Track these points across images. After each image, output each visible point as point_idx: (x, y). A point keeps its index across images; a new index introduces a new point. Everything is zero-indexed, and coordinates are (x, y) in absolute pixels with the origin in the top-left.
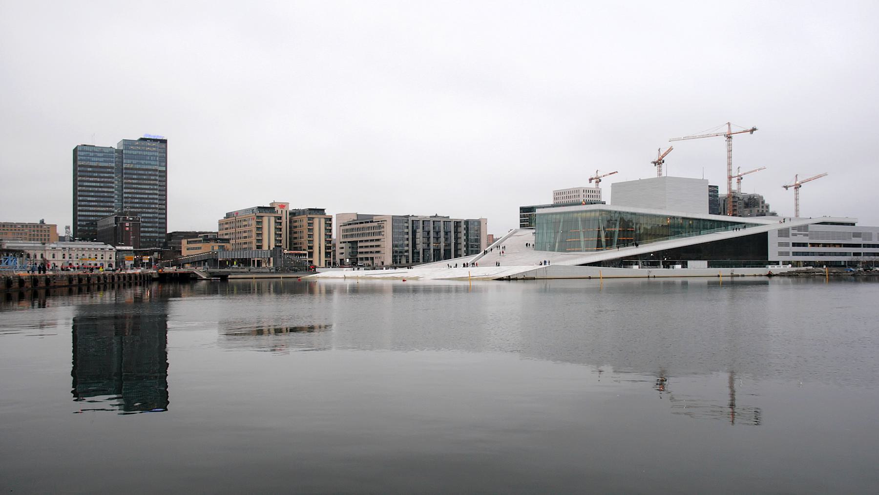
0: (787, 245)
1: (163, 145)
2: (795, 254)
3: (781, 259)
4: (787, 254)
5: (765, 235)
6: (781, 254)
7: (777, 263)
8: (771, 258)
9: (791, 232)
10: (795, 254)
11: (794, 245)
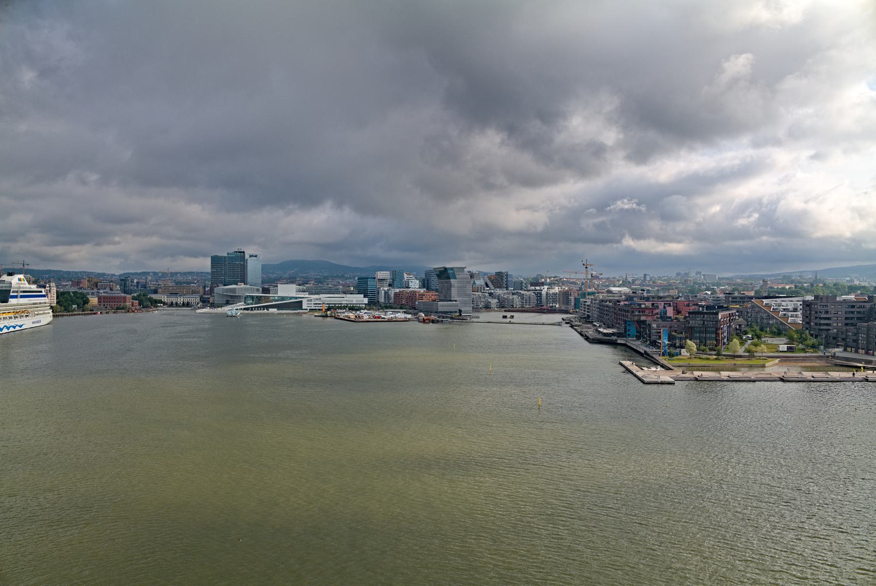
0: (312, 304)
1: (242, 254)
2: (314, 307)
3: (308, 308)
4: (311, 307)
5: (302, 301)
6: (308, 307)
7: (307, 309)
8: (303, 308)
9: (313, 300)
10: (314, 307)
11: (314, 304)
